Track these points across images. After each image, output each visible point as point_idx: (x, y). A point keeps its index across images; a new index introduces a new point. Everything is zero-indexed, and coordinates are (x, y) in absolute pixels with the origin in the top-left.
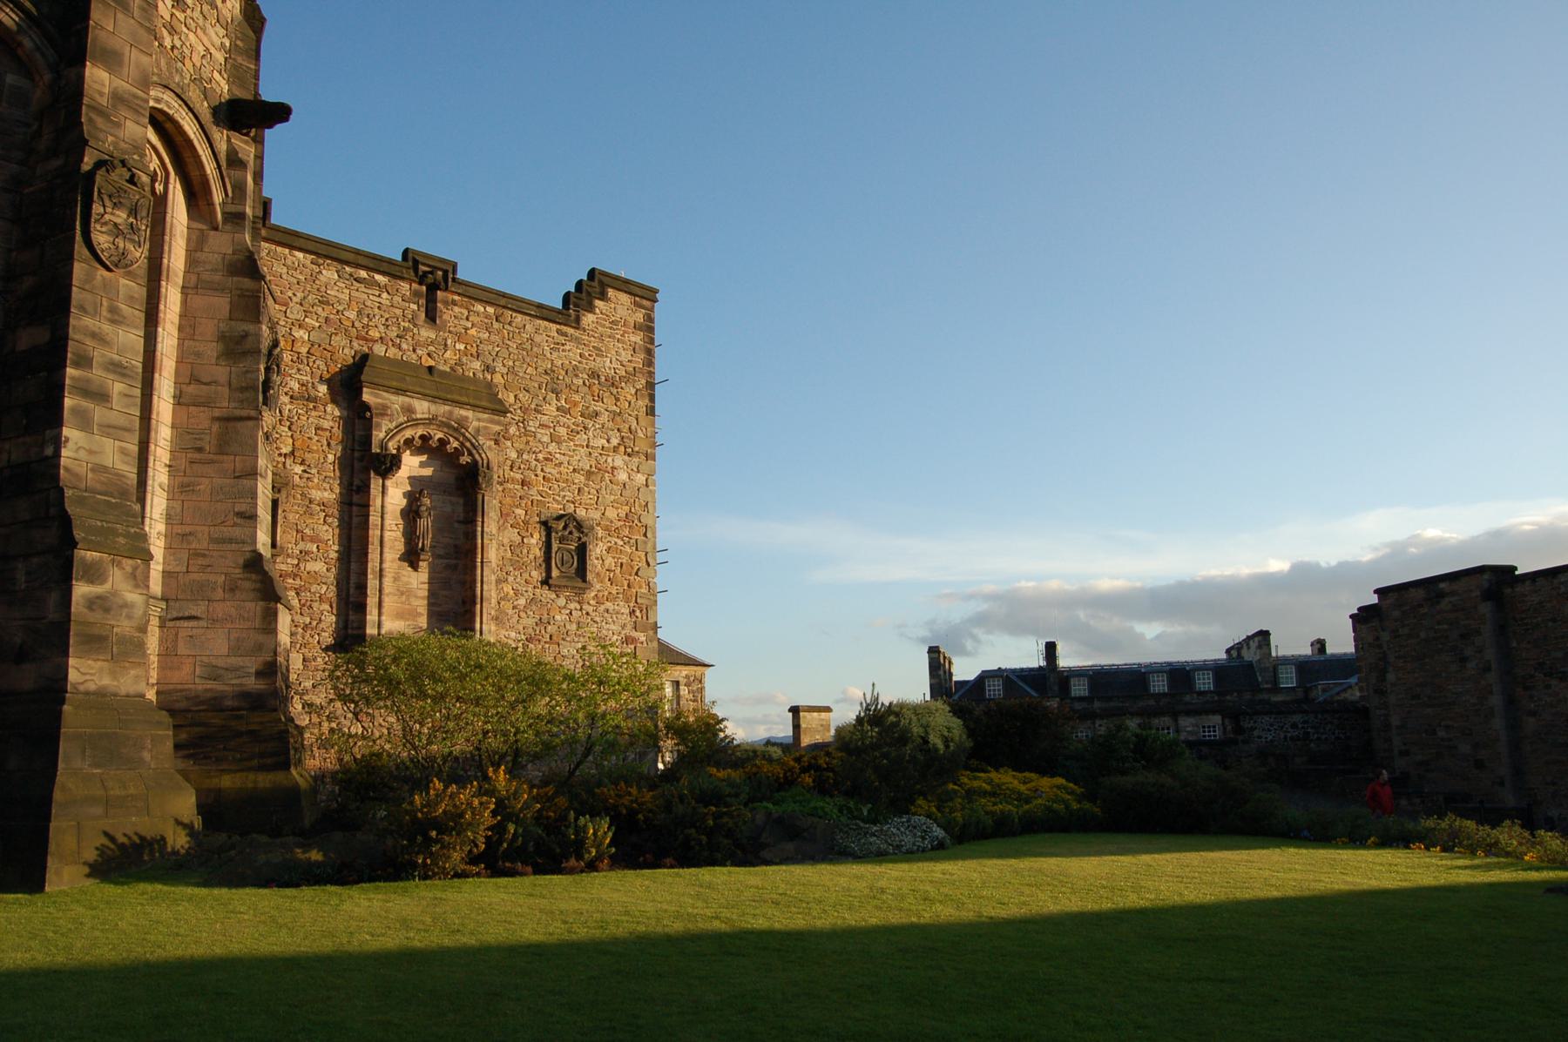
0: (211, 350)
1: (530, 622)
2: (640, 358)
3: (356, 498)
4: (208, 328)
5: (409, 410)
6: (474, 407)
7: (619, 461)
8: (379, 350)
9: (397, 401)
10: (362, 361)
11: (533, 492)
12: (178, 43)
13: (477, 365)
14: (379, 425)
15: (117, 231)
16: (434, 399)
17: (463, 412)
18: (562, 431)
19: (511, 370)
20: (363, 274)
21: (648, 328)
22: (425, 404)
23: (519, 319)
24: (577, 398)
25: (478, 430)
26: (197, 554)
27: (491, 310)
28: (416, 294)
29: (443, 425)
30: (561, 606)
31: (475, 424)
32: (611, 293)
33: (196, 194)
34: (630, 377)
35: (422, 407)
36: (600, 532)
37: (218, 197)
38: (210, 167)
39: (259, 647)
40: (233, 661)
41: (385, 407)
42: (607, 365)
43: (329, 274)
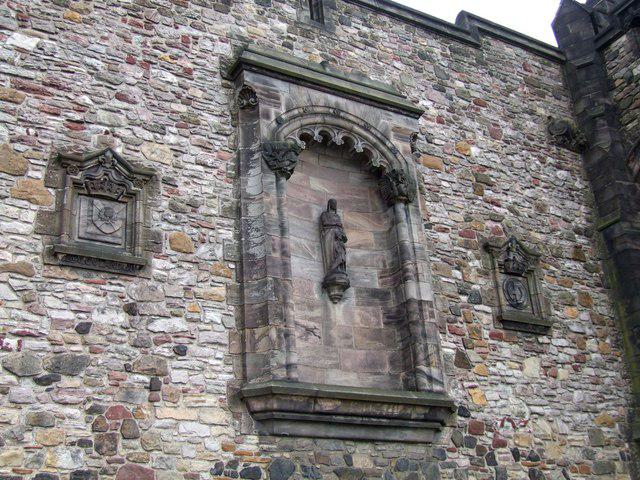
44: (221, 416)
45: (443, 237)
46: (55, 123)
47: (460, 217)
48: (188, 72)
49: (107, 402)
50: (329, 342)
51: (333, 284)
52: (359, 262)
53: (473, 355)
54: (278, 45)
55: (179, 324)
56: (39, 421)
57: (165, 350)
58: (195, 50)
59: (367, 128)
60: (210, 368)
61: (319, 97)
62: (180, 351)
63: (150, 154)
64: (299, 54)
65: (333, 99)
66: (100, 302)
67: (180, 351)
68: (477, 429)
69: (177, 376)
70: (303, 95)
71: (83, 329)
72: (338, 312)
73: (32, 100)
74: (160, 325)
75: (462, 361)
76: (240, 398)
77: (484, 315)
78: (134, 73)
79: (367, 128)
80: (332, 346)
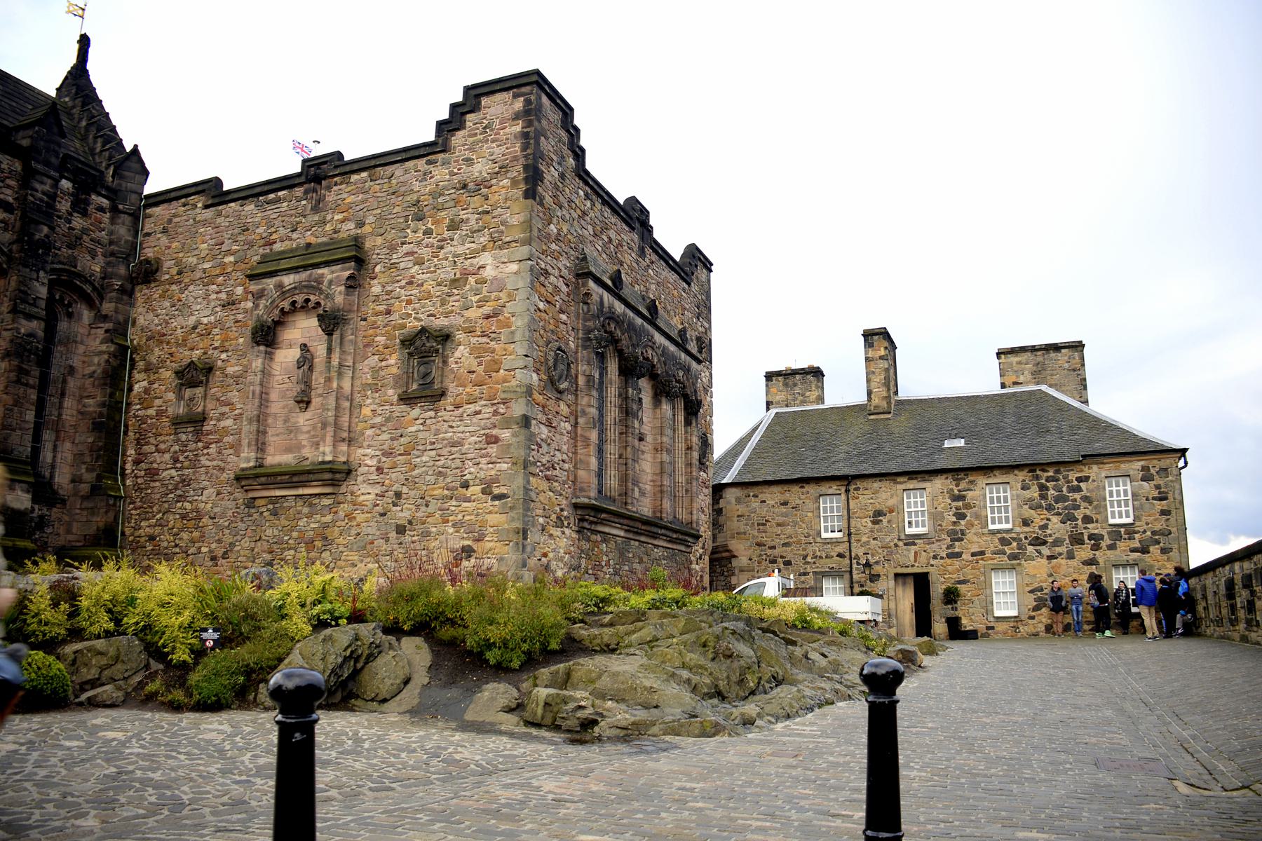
1: (385, 436)
2: (518, 147)
5: (280, 286)
6: (327, 264)
7: (486, 258)
8: (278, 247)
9: (270, 283)
11: (395, 316)
16: (295, 269)
17: (320, 271)
18: (426, 253)
19: (380, 218)
20: (272, 196)
22: (292, 276)
23: (390, 169)
24: (443, 214)
25: (331, 282)
27: (364, 174)
28: (306, 192)
31: (329, 277)
32: (484, 101)
35: (288, 280)
36: (460, 336)
41: (263, 290)
42: (481, 169)
43: (250, 207)
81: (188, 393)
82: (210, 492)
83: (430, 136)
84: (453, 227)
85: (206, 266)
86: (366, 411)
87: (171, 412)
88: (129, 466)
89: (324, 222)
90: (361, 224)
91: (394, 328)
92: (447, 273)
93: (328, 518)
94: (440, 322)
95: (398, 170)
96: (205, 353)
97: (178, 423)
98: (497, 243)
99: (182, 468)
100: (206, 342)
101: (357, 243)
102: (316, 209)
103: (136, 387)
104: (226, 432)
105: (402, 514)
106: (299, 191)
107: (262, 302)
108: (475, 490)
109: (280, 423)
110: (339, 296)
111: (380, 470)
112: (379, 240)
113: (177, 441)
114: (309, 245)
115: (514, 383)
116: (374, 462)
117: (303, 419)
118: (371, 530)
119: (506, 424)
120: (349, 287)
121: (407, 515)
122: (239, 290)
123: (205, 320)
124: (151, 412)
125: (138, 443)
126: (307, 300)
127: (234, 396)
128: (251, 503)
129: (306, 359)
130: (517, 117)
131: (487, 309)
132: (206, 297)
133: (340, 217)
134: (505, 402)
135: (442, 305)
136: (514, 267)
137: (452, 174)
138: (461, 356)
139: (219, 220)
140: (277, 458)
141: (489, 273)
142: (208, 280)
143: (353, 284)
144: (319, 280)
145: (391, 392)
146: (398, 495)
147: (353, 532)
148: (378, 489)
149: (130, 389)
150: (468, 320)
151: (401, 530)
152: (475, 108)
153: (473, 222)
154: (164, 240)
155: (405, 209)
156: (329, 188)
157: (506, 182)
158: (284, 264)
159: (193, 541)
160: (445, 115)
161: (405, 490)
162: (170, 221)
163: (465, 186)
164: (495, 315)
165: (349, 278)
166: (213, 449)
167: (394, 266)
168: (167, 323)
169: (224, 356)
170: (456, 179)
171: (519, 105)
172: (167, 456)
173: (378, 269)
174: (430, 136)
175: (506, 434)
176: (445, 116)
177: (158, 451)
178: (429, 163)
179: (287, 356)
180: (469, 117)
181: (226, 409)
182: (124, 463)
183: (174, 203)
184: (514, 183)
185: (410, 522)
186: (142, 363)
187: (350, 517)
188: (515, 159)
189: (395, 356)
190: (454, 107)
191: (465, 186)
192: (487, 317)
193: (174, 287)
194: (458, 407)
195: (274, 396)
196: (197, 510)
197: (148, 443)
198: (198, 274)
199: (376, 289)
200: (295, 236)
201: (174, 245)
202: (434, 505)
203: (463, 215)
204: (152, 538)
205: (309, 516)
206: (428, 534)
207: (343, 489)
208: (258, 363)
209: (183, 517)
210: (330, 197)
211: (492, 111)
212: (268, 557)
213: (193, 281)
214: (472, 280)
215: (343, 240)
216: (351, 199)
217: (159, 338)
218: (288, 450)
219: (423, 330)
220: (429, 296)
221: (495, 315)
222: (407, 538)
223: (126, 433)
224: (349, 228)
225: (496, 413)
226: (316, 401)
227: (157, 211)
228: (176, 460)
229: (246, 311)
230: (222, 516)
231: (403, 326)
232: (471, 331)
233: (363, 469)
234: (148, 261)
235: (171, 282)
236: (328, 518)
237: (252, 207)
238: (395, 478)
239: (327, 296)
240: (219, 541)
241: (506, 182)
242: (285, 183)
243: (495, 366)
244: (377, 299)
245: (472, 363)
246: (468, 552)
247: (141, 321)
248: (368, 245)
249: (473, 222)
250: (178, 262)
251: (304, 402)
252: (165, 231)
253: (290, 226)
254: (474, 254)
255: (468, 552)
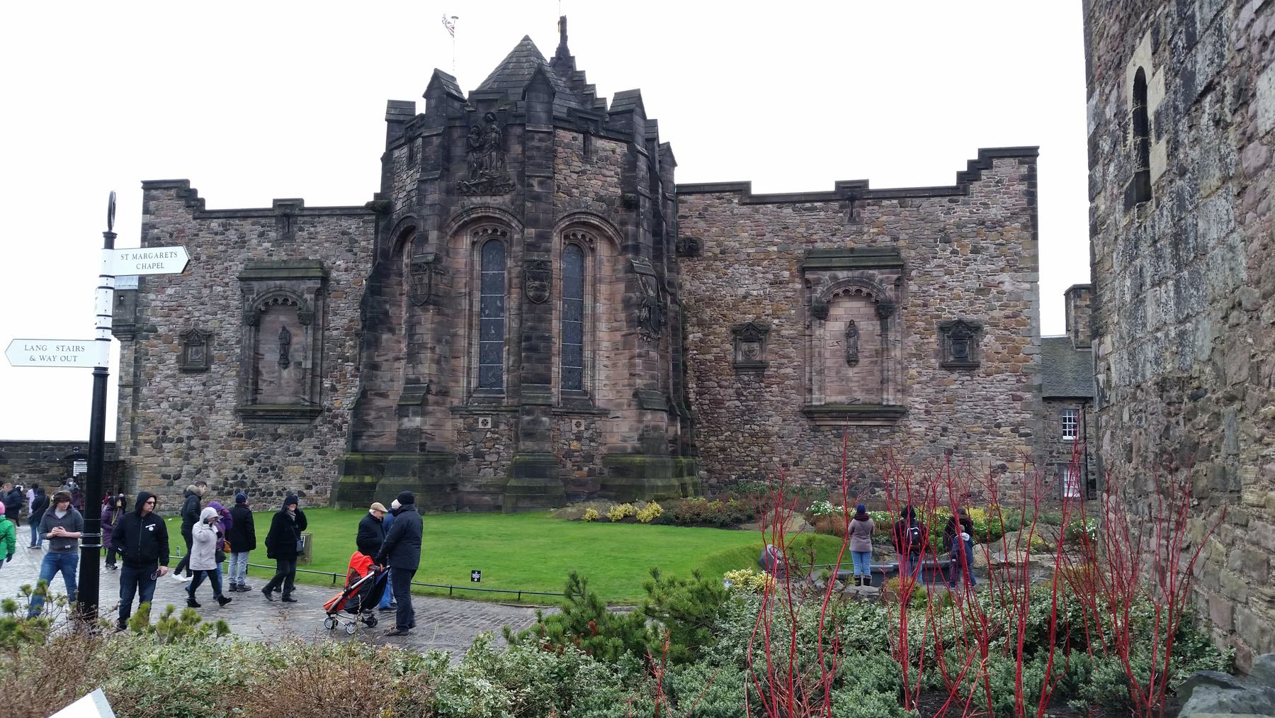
0: (620, 306)
2: (1025, 201)
3: (807, 332)
4: (619, 297)
5: (835, 278)
7: (1005, 277)
8: (819, 245)
9: (826, 275)
10: (810, 254)
11: (932, 309)
12: (582, 189)
13: (888, 239)
14: (815, 291)
15: (537, 289)
17: (871, 272)
18: (955, 268)
19: (913, 238)
20: (808, 205)
21: (1031, 178)
23: (917, 201)
25: (881, 281)
26: (618, 392)
27: (895, 202)
28: (842, 207)
29: (860, 281)
30: (955, 382)
32: (995, 162)
33: (611, 241)
34: (1014, 216)
35: (842, 275)
36: (987, 328)
37: (617, 241)
38: (610, 232)
39: (638, 429)
40: (632, 434)
41: (819, 279)
42: (995, 212)
43: (788, 211)
44: (231, 417)
45: (335, 333)
46: (181, 320)
47: (346, 321)
48: (227, 284)
49: (196, 415)
50: (280, 385)
51: (285, 362)
52: (296, 350)
53: (338, 386)
54: (266, 256)
55: (219, 387)
56: (178, 422)
57: (214, 397)
58: (229, 272)
59: (294, 292)
60: (230, 401)
61: (271, 283)
62: (219, 397)
63: (210, 326)
64: (275, 258)
65: (278, 282)
66: (192, 382)
67: (219, 397)
68: (336, 416)
69: (217, 405)
70: (264, 284)
71: (190, 393)
72: (285, 373)
73: (174, 314)
74: (213, 389)
75: (333, 389)
76: (236, 411)
77: (349, 367)
78: (206, 292)
79: (294, 292)
80: (281, 387)
81: (744, 346)
82: (777, 419)
83: (952, 182)
84: (975, 251)
85: (750, 251)
86: (913, 372)
87: (730, 358)
88: (692, 396)
89: (861, 233)
90: (896, 239)
91: (932, 317)
92: (973, 283)
93: (887, 442)
94: (970, 317)
95: (926, 203)
96: (758, 317)
97: (737, 368)
98: (1012, 267)
99: (747, 400)
100: (759, 310)
101: (895, 252)
102: (852, 220)
103: (691, 336)
104: (786, 377)
105: (950, 441)
106: (836, 205)
107: (819, 289)
108: (1006, 430)
109: (833, 373)
110: (890, 292)
111: (927, 412)
112: (913, 253)
113: (740, 380)
114: (852, 250)
115: (1031, 363)
116: (923, 406)
117: (851, 372)
118: (926, 451)
119: (1028, 389)
120: (897, 286)
121: (953, 442)
122: (786, 274)
123: (755, 293)
124: (708, 357)
125: (699, 379)
126: (859, 291)
127: (791, 351)
128: (816, 429)
129: (852, 331)
130: (1023, 179)
131: (1008, 312)
132: (753, 274)
133: (875, 230)
134: (1026, 375)
135: (971, 304)
136: (1027, 286)
137: (971, 212)
138: (989, 341)
139: (757, 216)
140: (834, 397)
141: (1007, 287)
142: (752, 262)
143: (899, 284)
144: (871, 278)
145: (933, 361)
146: (945, 429)
147: (909, 452)
148: (926, 425)
149: (685, 338)
150: (992, 318)
151: (949, 452)
152: (989, 166)
153: (992, 250)
154: (702, 224)
155: (935, 233)
156: (863, 207)
157: (1017, 225)
158: (836, 262)
159: (764, 453)
160: (964, 168)
161: (950, 426)
162: (706, 209)
163: (983, 223)
164: (1014, 316)
165: (898, 279)
166: (775, 388)
167: (927, 273)
168: (714, 290)
169: (776, 321)
170: (975, 217)
171: (1024, 170)
172: (731, 391)
173: (914, 273)
174: (952, 182)
175: (1028, 395)
176: (964, 168)
177: (721, 387)
178: (950, 201)
179: (835, 327)
180: (983, 172)
181: (783, 361)
182: (688, 393)
183: (708, 196)
184: (1025, 227)
185: (956, 448)
186: (694, 319)
187: (905, 442)
188: (1024, 210)
189: (934, 337)
190: (971, 163)
191: (983, 223)
192: (1007, 317)
193: (718, 263)
194: (988, 375)
195: (827, 354)
196: (766, 431)
197: (710, 380)
198: (744, 257)
199: (913, 287)
200: (835, 239)
201: (714, 229)
202: (975, 438)
203: (983, 244)
204: (723, 450)
205: (870, 439)
206: (971, 456)
207: (899, 423)
208: (818, 332)
209: (751, 436)
210: (866, 214)
211: (1002, 170)
212: (836, 466)
213: (737, 261)
214: (994, 291)
215: (881, 250)
216: (884, 218)
217: (710, 302)
218: (841, 393)
219: (960, 322)
220: (960, 298)
221: (1014, 316)
222: (954, 458)
223: (685, 372)
224: (884, 241)
225: (1019, 381)
226: (863, 361)
227: (691, 198)
228: (739, 394)
229: (795, 291)
230: (790, 436)
231: (940, 317)
232: (995, 325)
233: (912, 411)
234: (691, 240)
235: (715, 258)
236: (887, 442)
237: (790, 210)
238: (941, 419)
239: (879, 290)
240: (789, 454)
241: (1017, 225)
242: (823, 197)
243: (1016, 350)
244: (915, 295)
245: (998, 346)
246: (1003, 468)
247: (688, 286)
248: (903, 254)
249: (992, 250)
250: (719, 244)
251: (852, 361)
252: (701, 216)
253: (829, 233)
254: (994, 273)
255: (1003, 468)
